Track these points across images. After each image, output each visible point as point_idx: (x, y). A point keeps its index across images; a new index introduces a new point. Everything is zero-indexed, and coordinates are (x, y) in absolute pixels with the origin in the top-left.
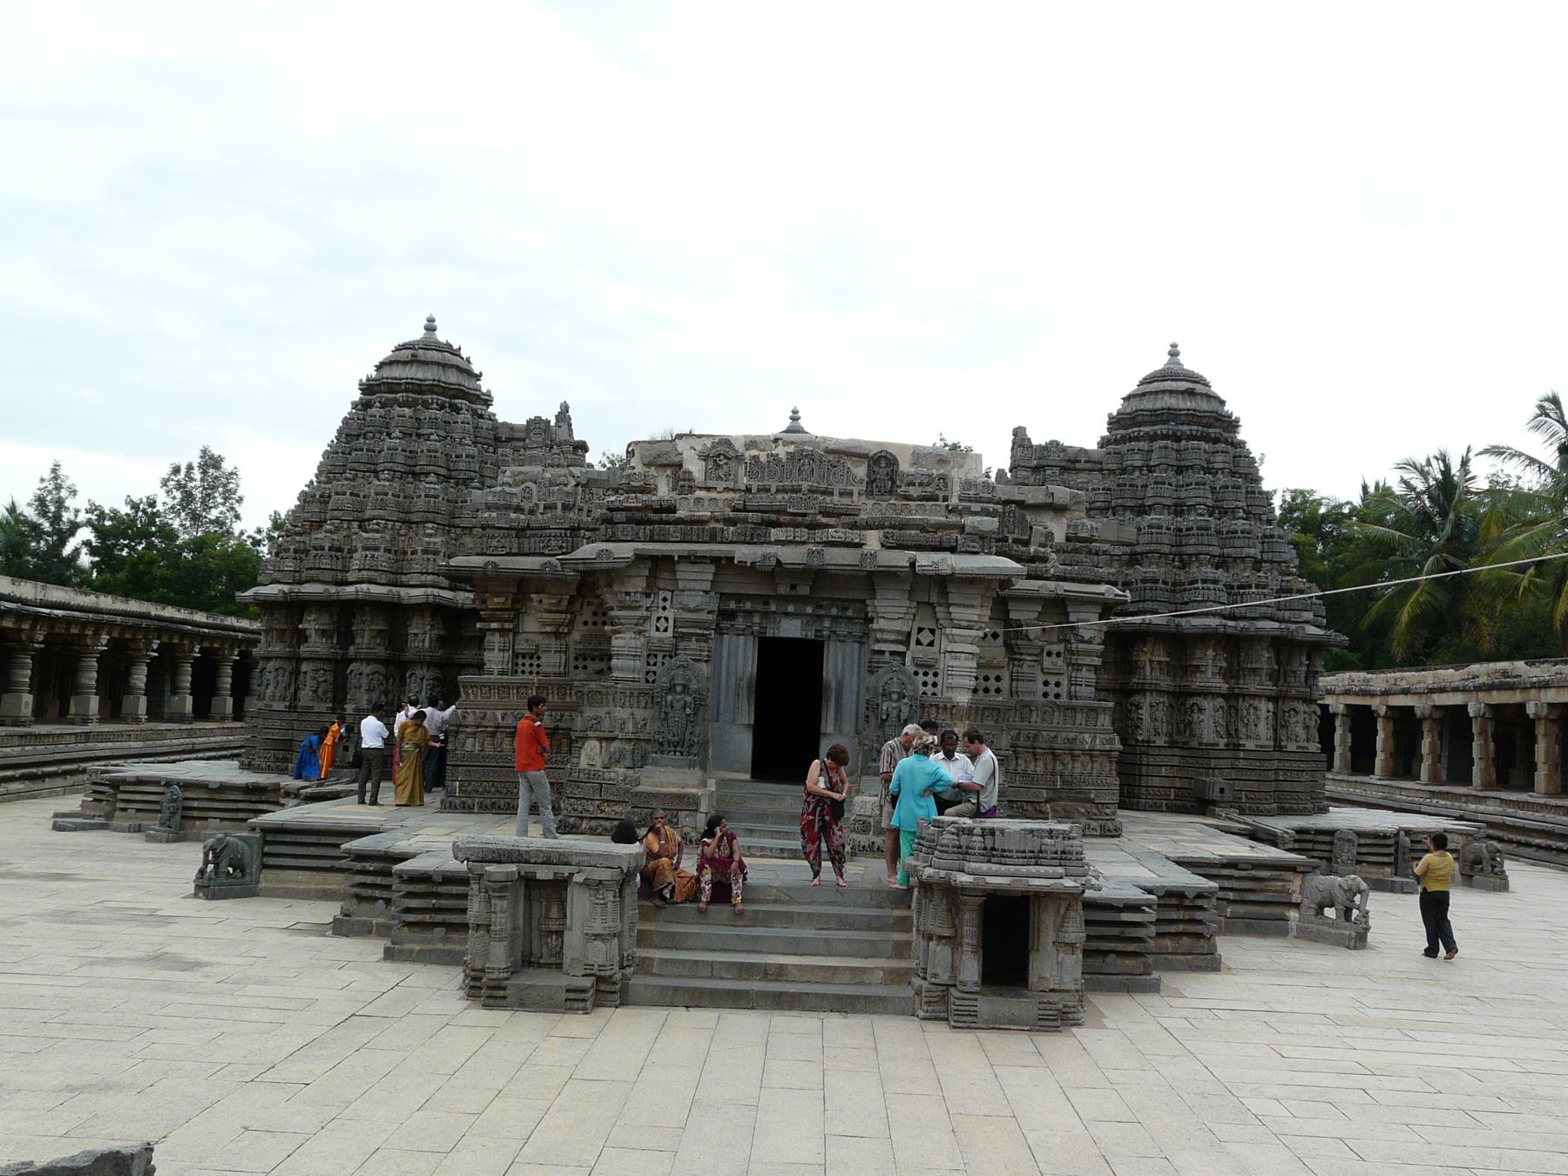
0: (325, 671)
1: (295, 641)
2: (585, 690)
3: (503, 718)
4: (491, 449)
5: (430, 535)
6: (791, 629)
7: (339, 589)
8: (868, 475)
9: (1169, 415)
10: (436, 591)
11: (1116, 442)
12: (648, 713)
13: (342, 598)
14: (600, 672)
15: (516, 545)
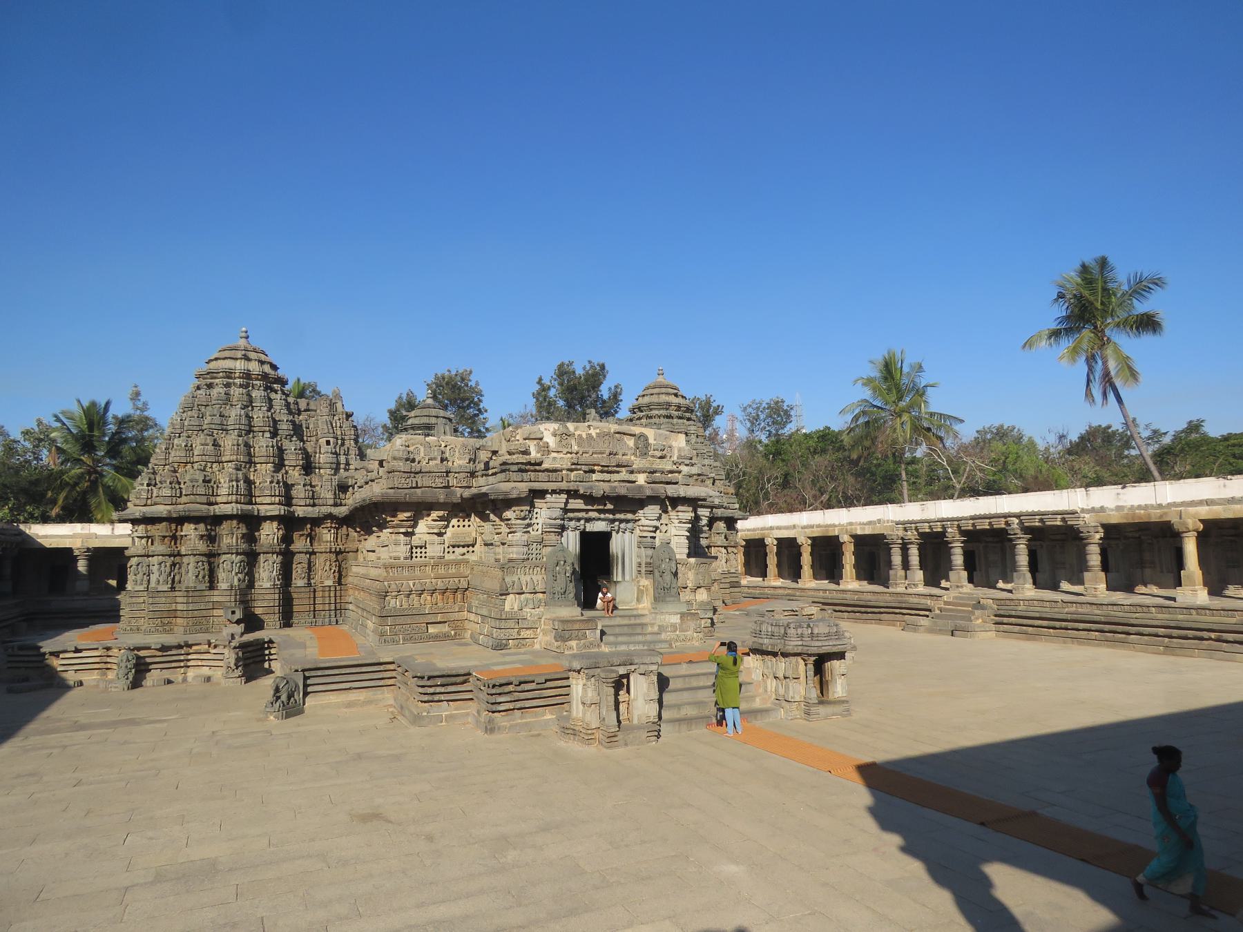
0: (203, 562)
1: (173, 543)
2: (507, 566)
3: (414, 586)
4: (296, 416)
5: (274, 472)
6: (600, 526)
7: (216, 507)
8: (635, 445)
9: (669, 405)
10: (286, 508)
11: (640, 419)
12: (540, 577)
13: (218, 514)
14: (464, 554)
15: (414, 482)
